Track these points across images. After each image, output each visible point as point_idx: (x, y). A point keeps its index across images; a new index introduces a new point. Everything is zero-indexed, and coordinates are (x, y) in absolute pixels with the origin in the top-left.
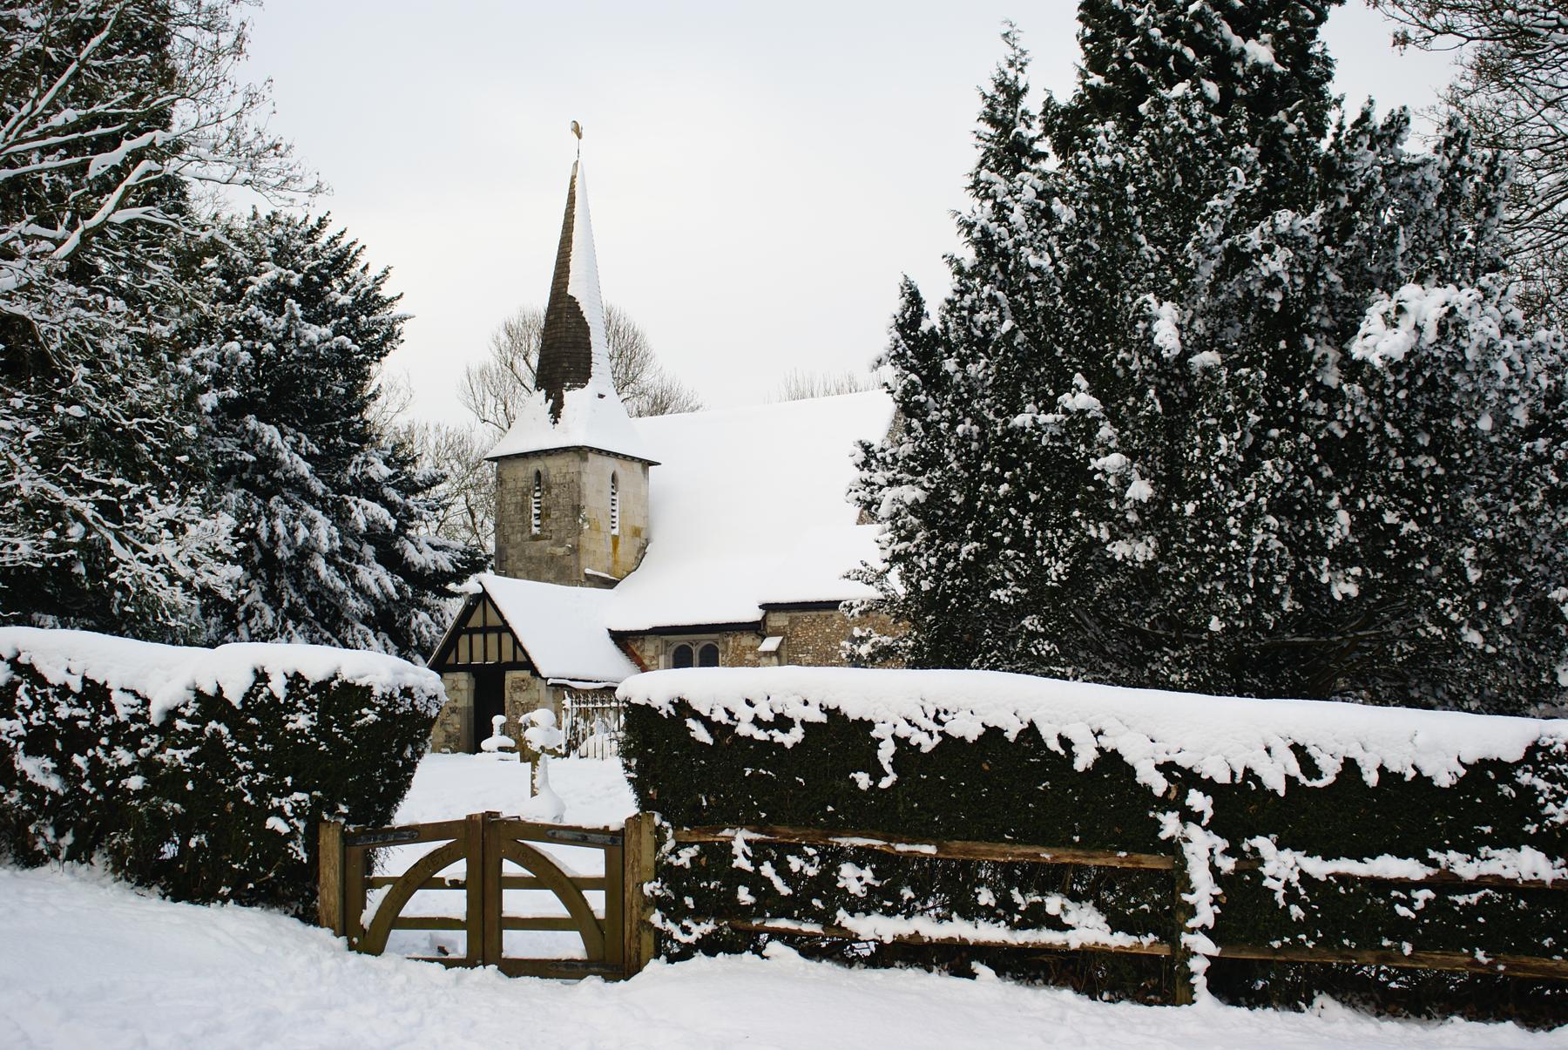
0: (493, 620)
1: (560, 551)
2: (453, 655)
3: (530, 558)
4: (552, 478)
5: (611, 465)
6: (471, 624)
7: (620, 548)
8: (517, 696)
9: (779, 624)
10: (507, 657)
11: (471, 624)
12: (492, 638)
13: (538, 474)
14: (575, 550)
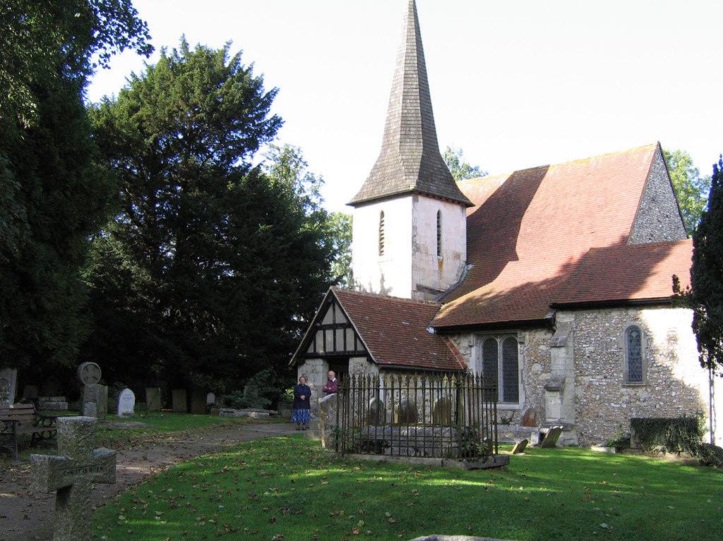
0: (340, 319)
2: (312, 345)
5: (435, 205)
6: (324, 323)
7: (444, 266)
9: (565, 321)
10: (350, 348)
12: (340, 332)
13: (382, 214)
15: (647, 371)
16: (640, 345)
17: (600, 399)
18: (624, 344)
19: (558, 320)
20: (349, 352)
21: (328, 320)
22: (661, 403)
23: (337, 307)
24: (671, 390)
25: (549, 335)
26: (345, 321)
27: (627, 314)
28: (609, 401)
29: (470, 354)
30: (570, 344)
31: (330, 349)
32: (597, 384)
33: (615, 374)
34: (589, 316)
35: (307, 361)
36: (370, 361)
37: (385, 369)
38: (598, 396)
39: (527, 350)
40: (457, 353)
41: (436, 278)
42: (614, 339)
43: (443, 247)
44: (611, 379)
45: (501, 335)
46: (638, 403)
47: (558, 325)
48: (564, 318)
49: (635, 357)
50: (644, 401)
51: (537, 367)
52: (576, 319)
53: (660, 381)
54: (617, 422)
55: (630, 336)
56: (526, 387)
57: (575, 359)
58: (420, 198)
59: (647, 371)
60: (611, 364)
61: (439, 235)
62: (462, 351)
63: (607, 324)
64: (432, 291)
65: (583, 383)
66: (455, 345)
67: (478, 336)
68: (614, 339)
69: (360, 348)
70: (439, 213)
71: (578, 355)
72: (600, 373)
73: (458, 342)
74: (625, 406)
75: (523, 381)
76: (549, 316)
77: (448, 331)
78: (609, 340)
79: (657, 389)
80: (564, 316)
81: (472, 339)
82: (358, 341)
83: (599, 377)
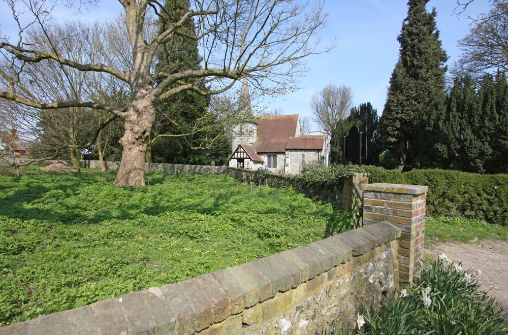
0: (242, 150)
10: (245, 157)
12: (242, 154)
31: (239, 157)
36: (251, 160)
69: (248, 157)
71: (291, 159)
76: (284, 151)
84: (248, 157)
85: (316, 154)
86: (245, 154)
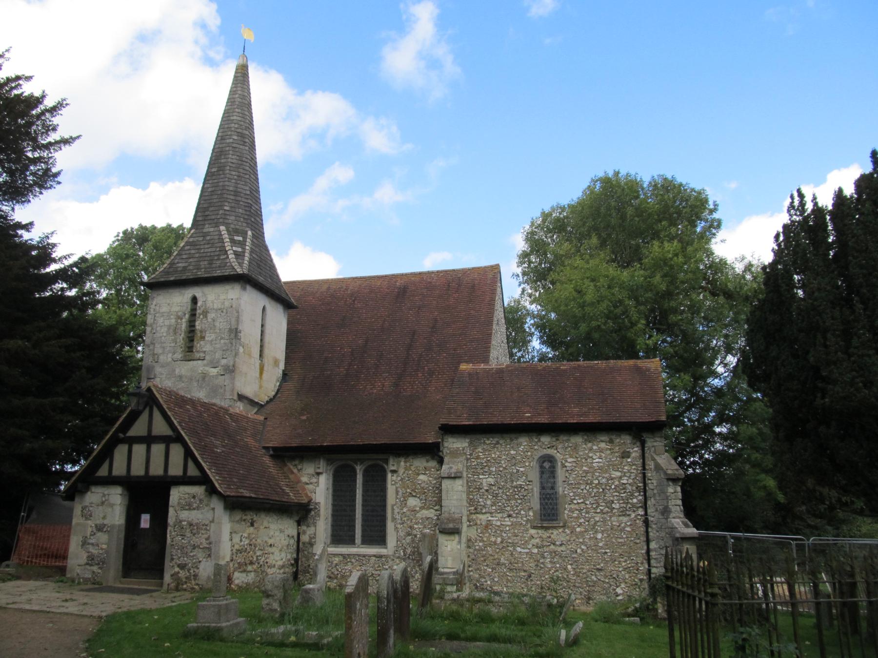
1: (214, 371)
3: (181, 377)
4: (209, 304)
7: (265, 375)
8: (184, 515)
9: (455, 446)
10: (175, 470)
11: (133, 432)
12: (158, 449)
13: (194, 300)
14: (230, 370)
15: (565, 509)
16: (554, 477)
17: (502, 542)
18: (534, 475)
19: (446, 444)
20: (175, 477)
21: (138, 429)
22: (583, 547)
23: (157, 414)
24: (596, 532)
25: (433, 464)
26: (168, 432)
27: (539, 441)
28: (514, 545)
29: (318, 485)
30: (465, 474)
32: (499, 523)
33: (522, 512)
34: (490, 441)
35: (93, 489)
36: (212, 491)
37: (236, 505)
38: (499, 540)
39: (402, 480)
40: (299, 481)
41: (256, 387)
42: (522, 469)
43: (266, 351)
44: (516, 517)
45: (362, 461)
46: (552, 547)
47: (445, 451)
48: (453, 444)
49: (549, 491)
50: (561, 545)
51: (412, 502)
52: (470, 443)
53: (582, 520)
54: (525, 571)
55: (541, 467)
56: (399, 526)
57: (468, 494)
58: (248, 287)
59: (565, 509)
60: (516, 499)
61: (262, 332)
62: (304, 479)
63: (512, 452)
64: (252, 402)
65: (479, 522)
66: (295, 471)
67: (329, 462)
68: (522, 469)
69: (193, 471)
70: (264, 309)
71: (473, 488)
72: (502, 510)
73: (299, 467)
74: (535, 551)
75: (394, 519)
77: (284, 454)
78: (515, 471)
79: (578, 529)
80: (455, 440)
81: (322, 465)
82: (191, 464)
83: (500, 515)
84: (193, 471)
85: (625, 455)
86: (177, 452)
